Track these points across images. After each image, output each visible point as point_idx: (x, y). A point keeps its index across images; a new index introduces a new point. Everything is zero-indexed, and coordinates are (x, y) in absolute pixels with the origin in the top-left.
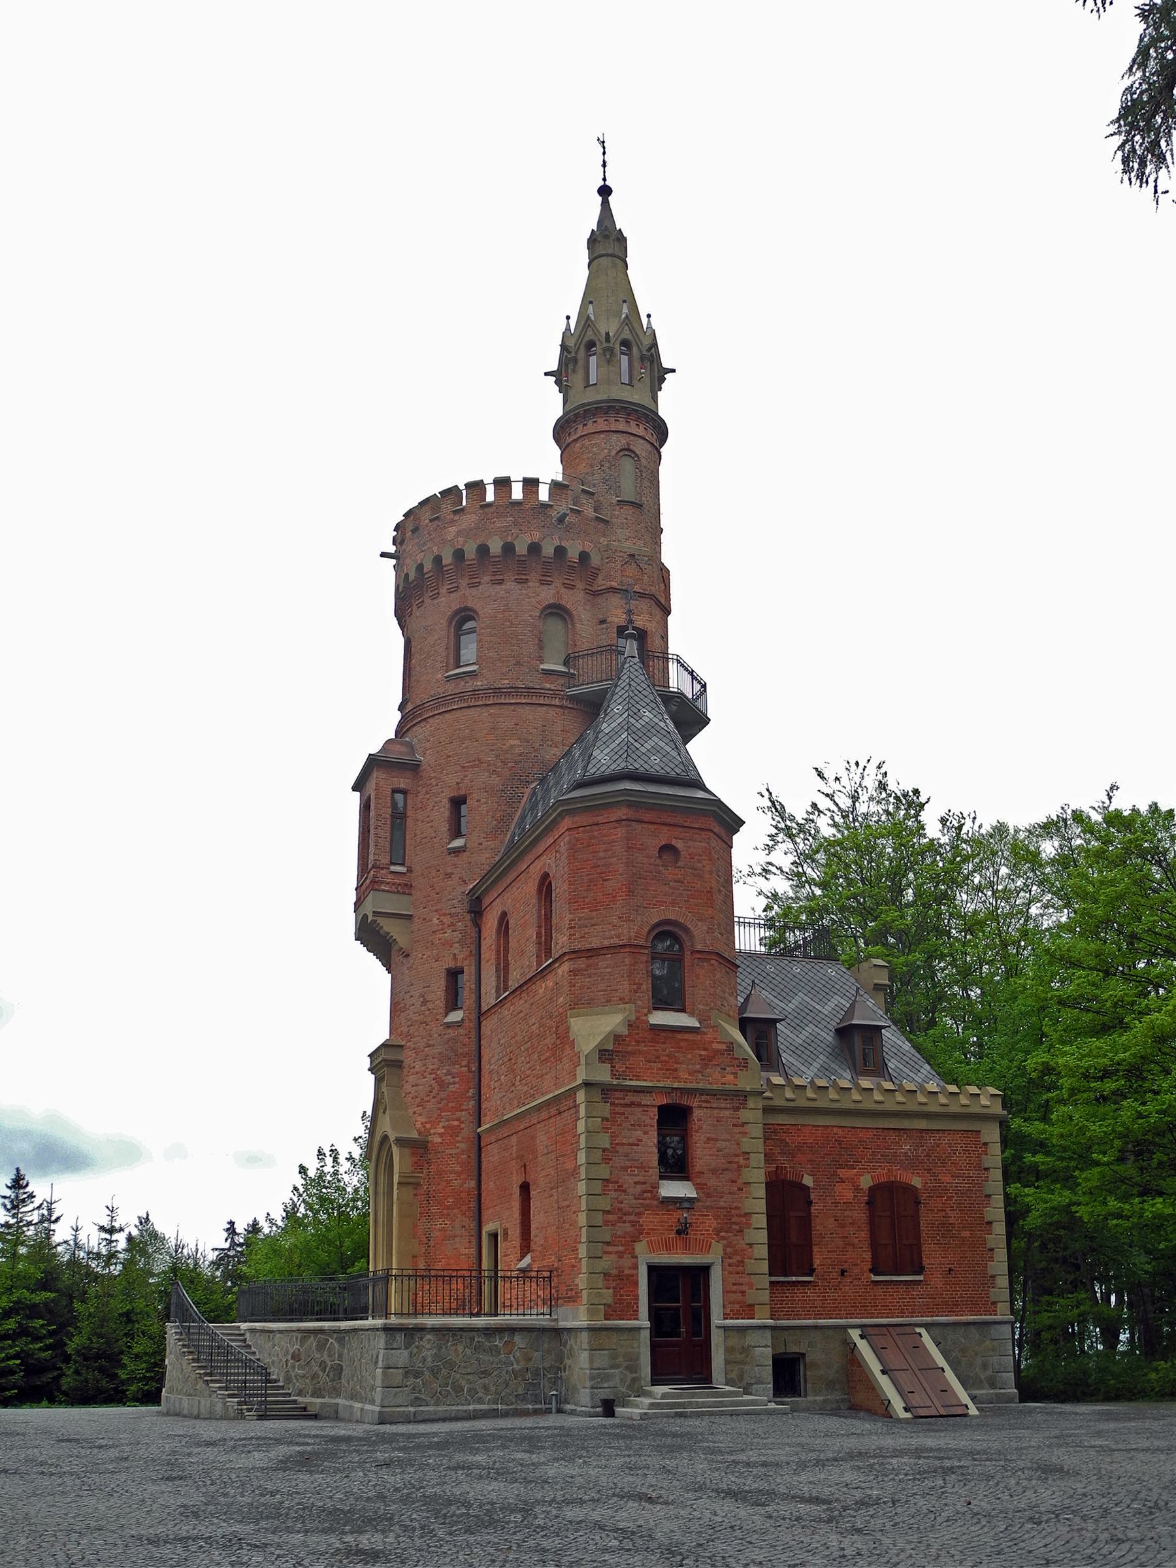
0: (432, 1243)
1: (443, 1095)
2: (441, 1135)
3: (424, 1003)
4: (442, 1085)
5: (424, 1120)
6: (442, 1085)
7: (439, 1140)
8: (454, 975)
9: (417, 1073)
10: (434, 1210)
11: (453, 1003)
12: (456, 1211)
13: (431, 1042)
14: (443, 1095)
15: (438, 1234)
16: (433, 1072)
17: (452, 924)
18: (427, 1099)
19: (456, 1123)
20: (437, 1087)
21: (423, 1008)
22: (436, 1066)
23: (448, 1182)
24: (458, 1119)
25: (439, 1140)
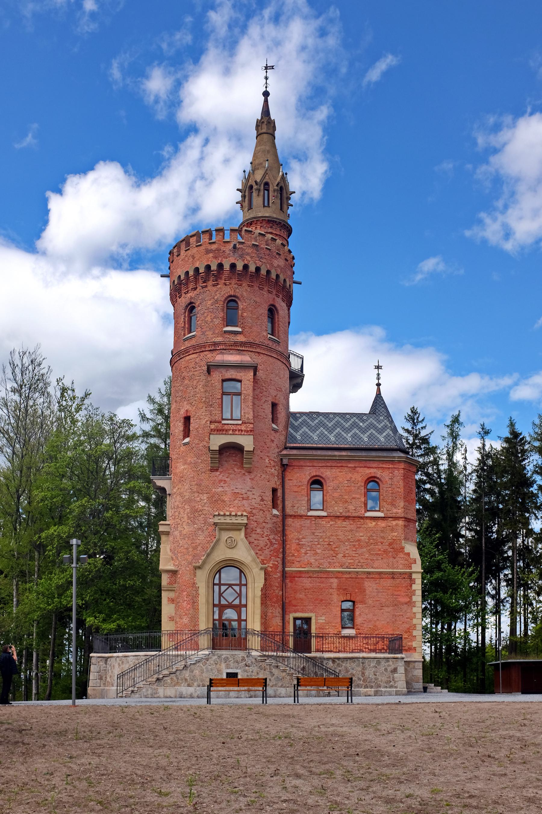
0: (267, 618)
1: (272, 548)
2: (271, 567)
3: (262, 500)
4: (272, 544)
5: (263, 558)
6: (271, 543)
7: (270, 570)
8: (274, 491)
9: (258, 534)
10: (268, 603)
11: (275, 506)
12: (277, 605)
13: (266, 521)
14: (272, 548)
15: (270, 614)
16: (267, 536)
17: (274, 466)
18: (265, 548)
19: (276, 563)
20: (269, 543)
21: (262, 503)
22: (269, 534)
23: (274, 590)
24: (277, 562)
25: (270, 570)
